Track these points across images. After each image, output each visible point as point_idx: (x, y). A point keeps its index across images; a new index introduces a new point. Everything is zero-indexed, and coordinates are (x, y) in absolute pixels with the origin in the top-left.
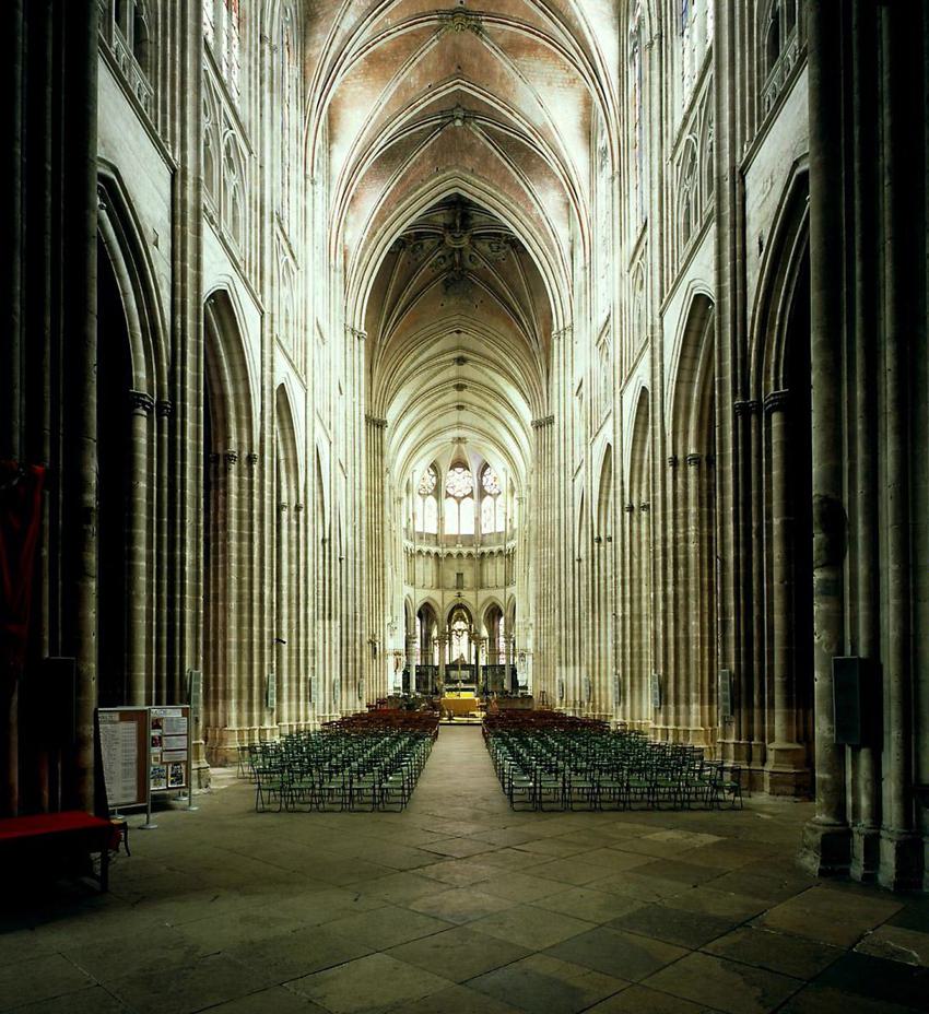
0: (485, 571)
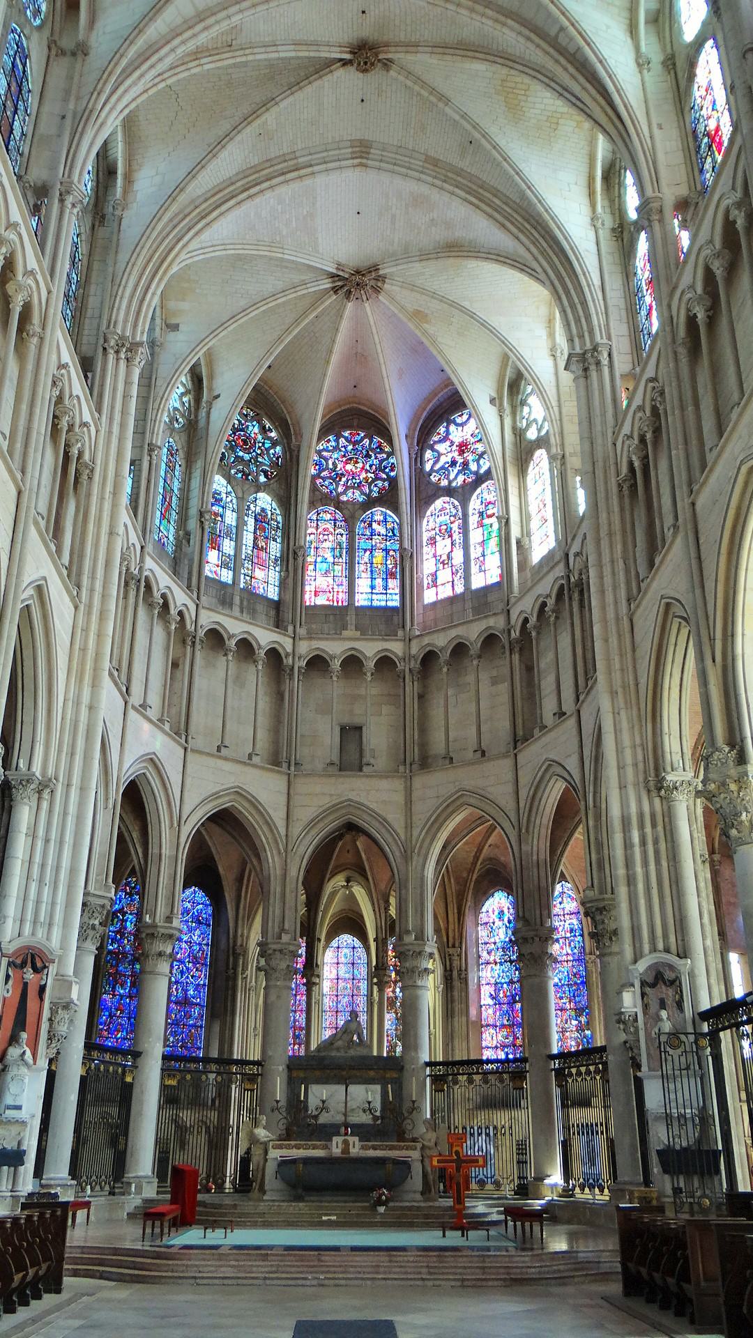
0: (437, 712)
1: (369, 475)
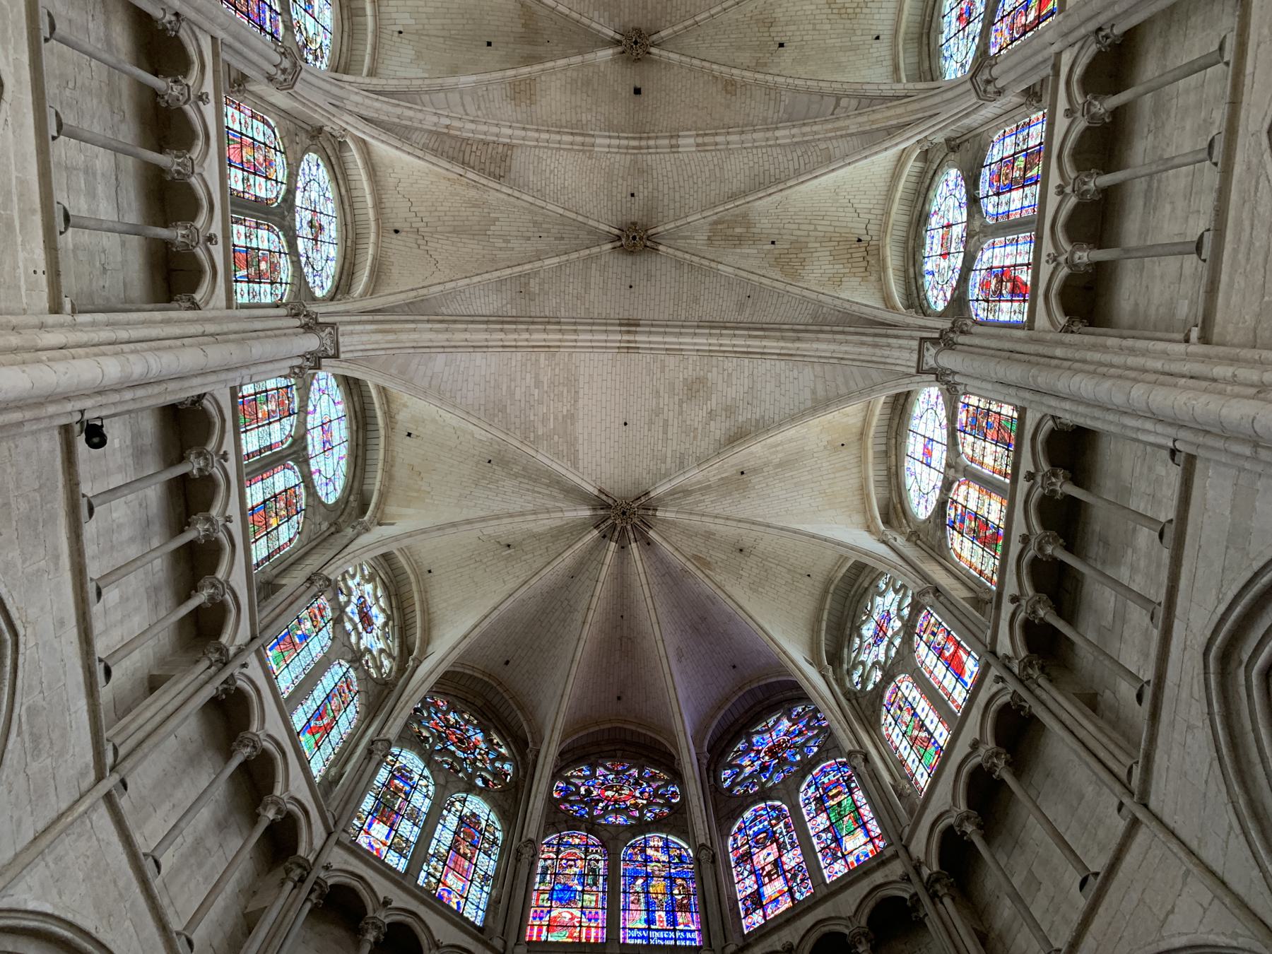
1: (640, 801)
